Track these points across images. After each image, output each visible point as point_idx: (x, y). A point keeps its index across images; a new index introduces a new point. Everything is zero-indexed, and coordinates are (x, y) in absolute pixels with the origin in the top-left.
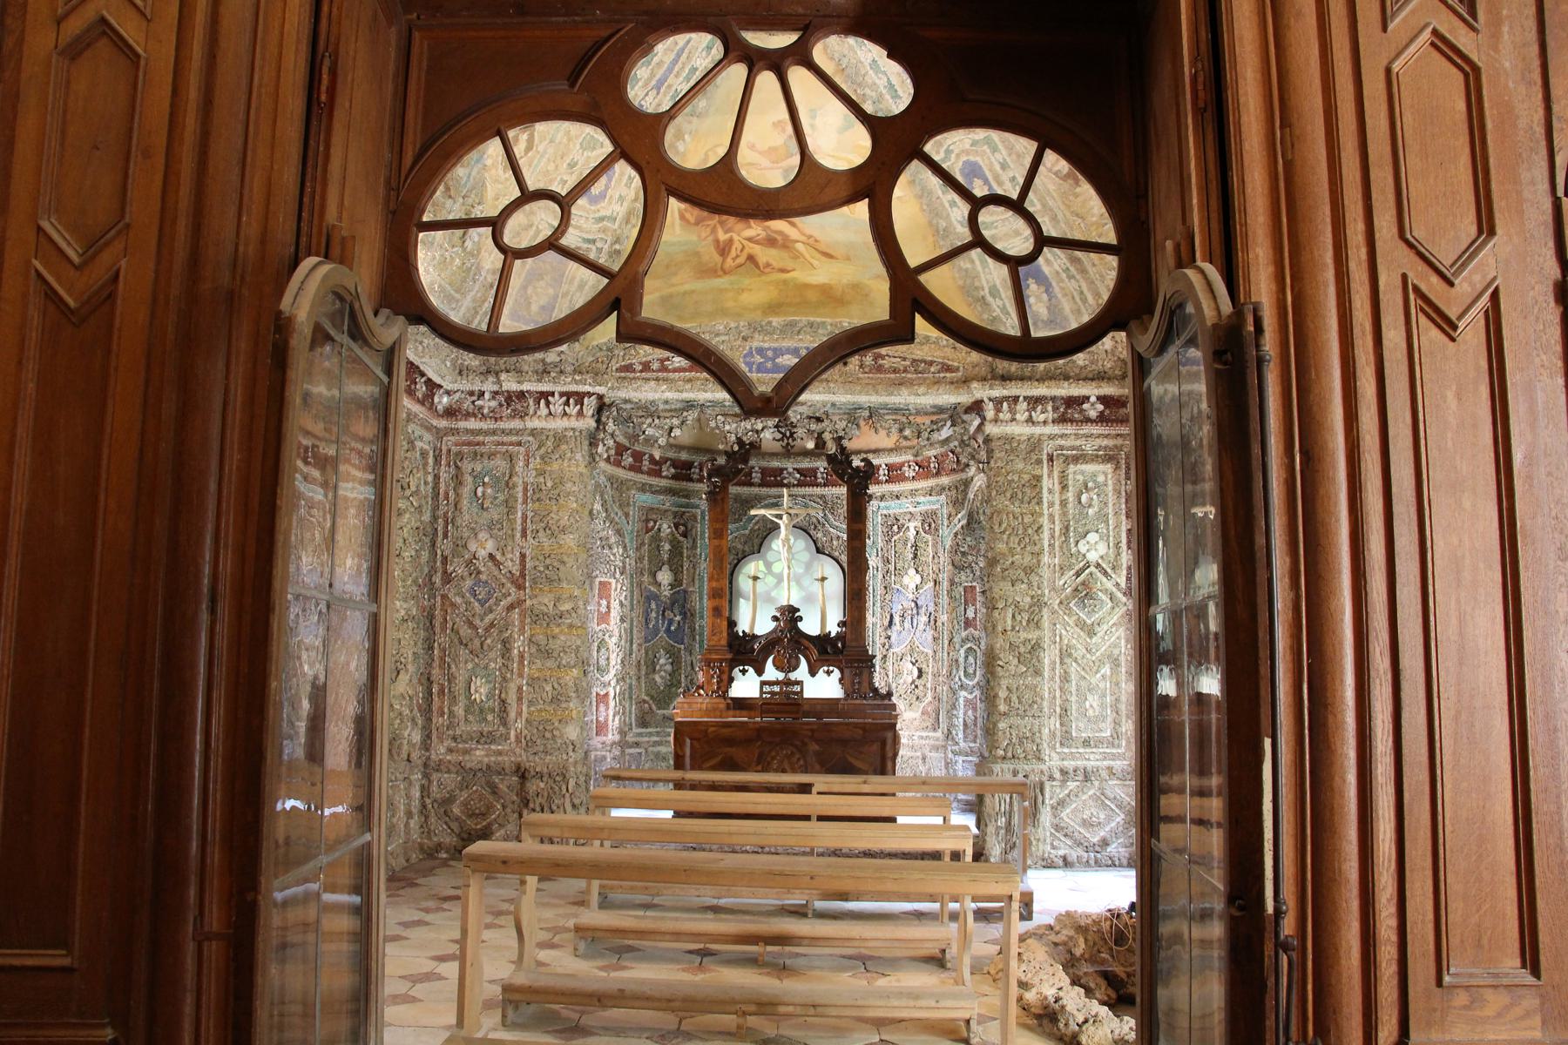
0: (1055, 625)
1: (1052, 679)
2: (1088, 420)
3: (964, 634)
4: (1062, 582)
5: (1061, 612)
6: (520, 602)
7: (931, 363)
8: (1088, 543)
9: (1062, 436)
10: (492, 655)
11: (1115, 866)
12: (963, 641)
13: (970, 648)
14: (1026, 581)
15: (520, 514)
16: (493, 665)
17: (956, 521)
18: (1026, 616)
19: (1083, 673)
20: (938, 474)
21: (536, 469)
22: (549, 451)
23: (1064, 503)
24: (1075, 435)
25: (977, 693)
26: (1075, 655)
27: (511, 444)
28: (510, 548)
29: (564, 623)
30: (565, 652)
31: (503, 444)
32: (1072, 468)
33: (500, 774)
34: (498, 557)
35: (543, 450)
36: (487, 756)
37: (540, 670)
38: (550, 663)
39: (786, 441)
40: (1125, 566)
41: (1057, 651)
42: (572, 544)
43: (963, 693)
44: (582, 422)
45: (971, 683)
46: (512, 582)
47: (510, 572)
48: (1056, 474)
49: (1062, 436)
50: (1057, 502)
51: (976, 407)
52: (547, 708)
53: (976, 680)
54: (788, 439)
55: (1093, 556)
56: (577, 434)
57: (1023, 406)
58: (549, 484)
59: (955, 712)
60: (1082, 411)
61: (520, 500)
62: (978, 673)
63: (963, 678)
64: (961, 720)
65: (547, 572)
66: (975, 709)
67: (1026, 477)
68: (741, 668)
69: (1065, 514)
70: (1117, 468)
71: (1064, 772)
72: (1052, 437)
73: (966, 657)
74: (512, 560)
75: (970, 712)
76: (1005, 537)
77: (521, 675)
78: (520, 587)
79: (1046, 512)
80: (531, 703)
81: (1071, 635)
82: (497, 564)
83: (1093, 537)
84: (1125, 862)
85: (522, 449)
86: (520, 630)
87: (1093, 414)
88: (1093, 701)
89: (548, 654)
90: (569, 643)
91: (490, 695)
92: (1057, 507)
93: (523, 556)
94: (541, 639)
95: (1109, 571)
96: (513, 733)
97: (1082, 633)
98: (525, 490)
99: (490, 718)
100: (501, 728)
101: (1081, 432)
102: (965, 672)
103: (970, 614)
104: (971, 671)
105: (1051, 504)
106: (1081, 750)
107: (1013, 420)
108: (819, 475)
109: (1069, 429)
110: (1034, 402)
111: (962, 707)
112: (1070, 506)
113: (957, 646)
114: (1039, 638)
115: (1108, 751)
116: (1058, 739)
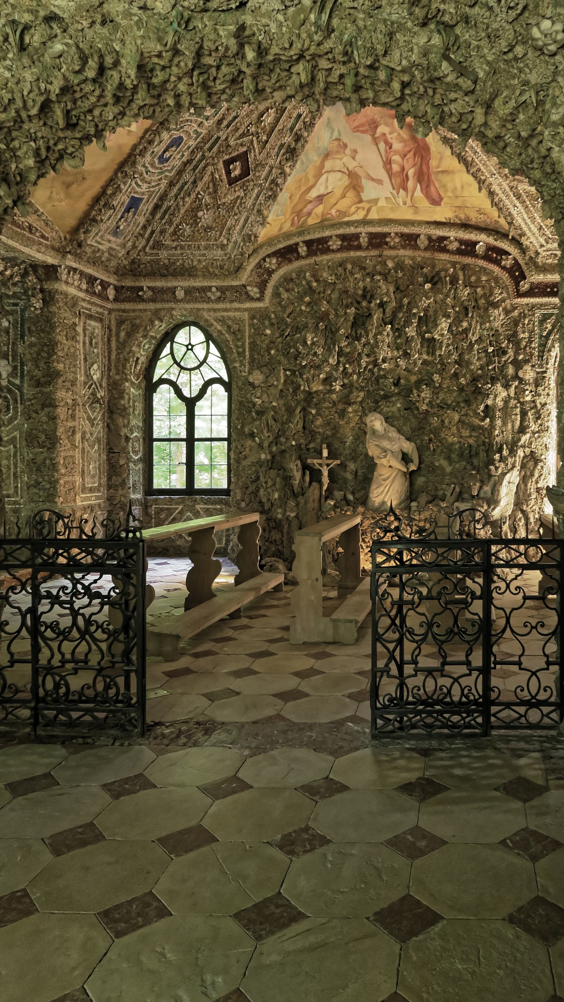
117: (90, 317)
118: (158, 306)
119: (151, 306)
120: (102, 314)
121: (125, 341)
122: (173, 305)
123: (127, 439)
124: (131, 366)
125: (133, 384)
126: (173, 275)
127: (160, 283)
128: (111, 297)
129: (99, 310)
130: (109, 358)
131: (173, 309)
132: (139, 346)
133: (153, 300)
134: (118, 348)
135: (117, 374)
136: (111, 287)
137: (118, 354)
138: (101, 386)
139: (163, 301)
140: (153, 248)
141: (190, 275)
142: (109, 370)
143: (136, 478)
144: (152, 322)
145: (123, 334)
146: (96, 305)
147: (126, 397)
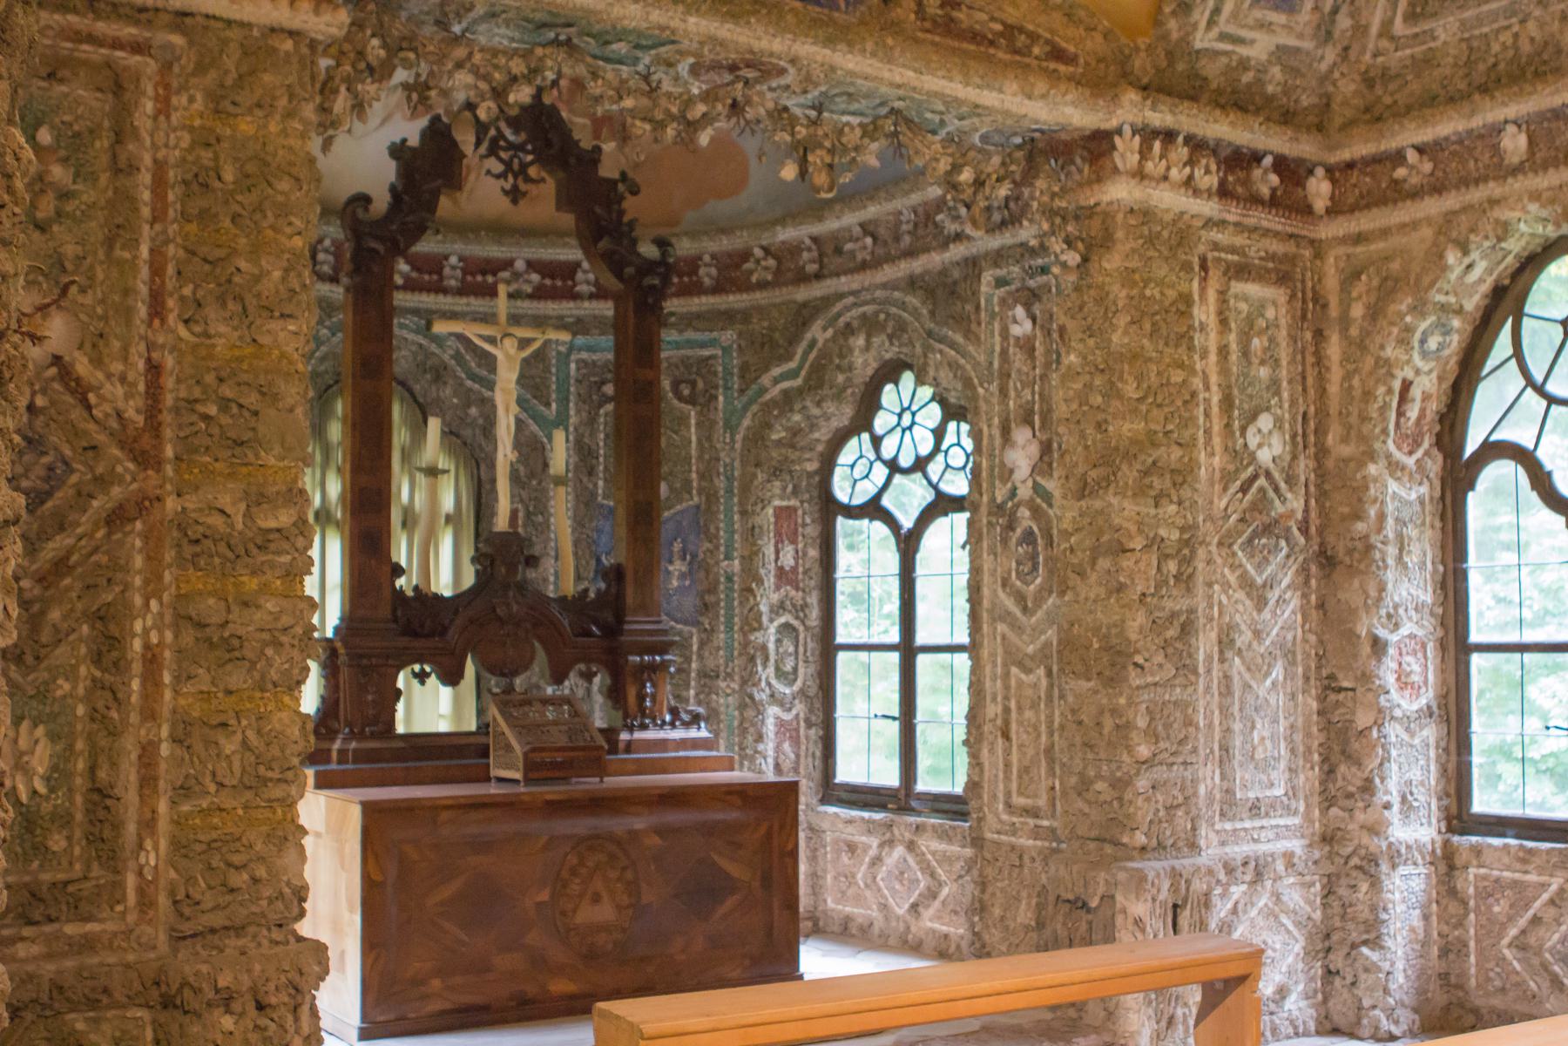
0: (1210, 585)
1: (1208, 689)
2: (1255, 200)
3: (775, 597)
4: (1223, 504)
5: (1219, 561)
6: (144, 504)
7: (1034, 37)
8: (1259, 431)
9: (1221, 224)
10: (61, 654)
11: (1297, 1034)
12: (771, 611)
13: (787, 627)
14: (1175, 499)
15: (144, 251)
16: (65, 686)
17: (765, 380)
18: (1172, 566)
19: (1247, 676)
20: (717, 289)
21: (191, 129)
22: (229, 82)
23: (1223, 351)
24: (1237, 224)
25: (799, 708)
26: (1238, 644)
27: (117, 44)
28: (116, 344)
29: (272, 565)
30: (278, 645)
31: (91, 39)
32: (1237, 287)
33: (93, 1004)
34: (82, 367)
35: (212, 76)
36: (49, 956)
37: (206, 696)
38: (237, 678)
39: (511, 179)
40: (1303, 478)
41: (1214, 635)
42: (289, 349)
43: (773, 711)
44: (327, 17)
45: (788, 691)
46: (122, 445)
47: (119, 415)
48: (1212, 295)
49: (1221, 224)
50: (1213, 349)
51: (1098, 144)
52: (228, 804)
53: (799, 683)
54: (516, 177)
55: (1265, 456)
56: (305, 51)
57: (1181, 152)
58: (229, 175)
59: (761, 747)
60: (1246, 182)
61: (146, 212)
62: (801, 671)
63: (774, 682)
64: (770, 761)
65: (225, 420)
66: (796, 741)
67: (1171, 294)
68: (417, 668)
69: (1224, 371)
70: (1293, 297)
71: (1230, 870)
72: (1210, 223)
73: (779, 641)
74: (123, 379)
75: (786, 746)
76: (1144, 408)
77: (149, 715)
78: (147, 459)
79: (1198, 367)
80: (184, 791)
81: (1240, 609)
82: (80, 391)
83: (1265, 422)
84: (1312, 1026)
85: (151, 66)
86: (147, 582)
87: (1265, 191)
88: (1262, 729)
89: (227, 649)
90: (286, 620)
91: (58, 775)
92: (1213, 358)
93: (154, 369)
94: (210, 608)
95: (1283, 485)
96: (131, 881)
97: (1248, 602)
98: (159, 185)
99: (57, 842)
100: (96, 871)
101: (1251, 221)
102: (777, 669)
103: (788, 560)
104: (788, 667)
105: (1204, 355)
106: (1247, 824)
107: (1166, 178)
108: (447, 271)
109: (1233, 214)
110: (1197, 145)
111: (771, 735)
112: (1234, 357)
113: (765, 619)
114: (1192, 611)
115: (1282, 822)
116: (1217, 807)
117: (1242, 271)
118: (1451, 201)
119: (1432, 207)
120: (1291, 259)
121: (1366, 334)
122: (1492, 189)
123: (1378, 646)
124: (1384, 408)
125: (1394, 467)
126: (1484, 89)
127: (1448, 126)
128: (1320, 205)
129: (1276, 247)
130: (1322, 392)
131: (1494, 202)
132: (1404, 342)
133: (1437, 188)
134: (1346, 359)
135: (1345, 440)
136: (1320, 172)
137: (1348, 377)
138: (1290, 480)
139: (1466, 182)
140: (1411, 17)
141: (1536, 74)
142: (1320, 431)
143: (1416, 774)
144: (1436, 258)
145: (1357, 311)
146: (1267, 233)
147: (1372, 512)
